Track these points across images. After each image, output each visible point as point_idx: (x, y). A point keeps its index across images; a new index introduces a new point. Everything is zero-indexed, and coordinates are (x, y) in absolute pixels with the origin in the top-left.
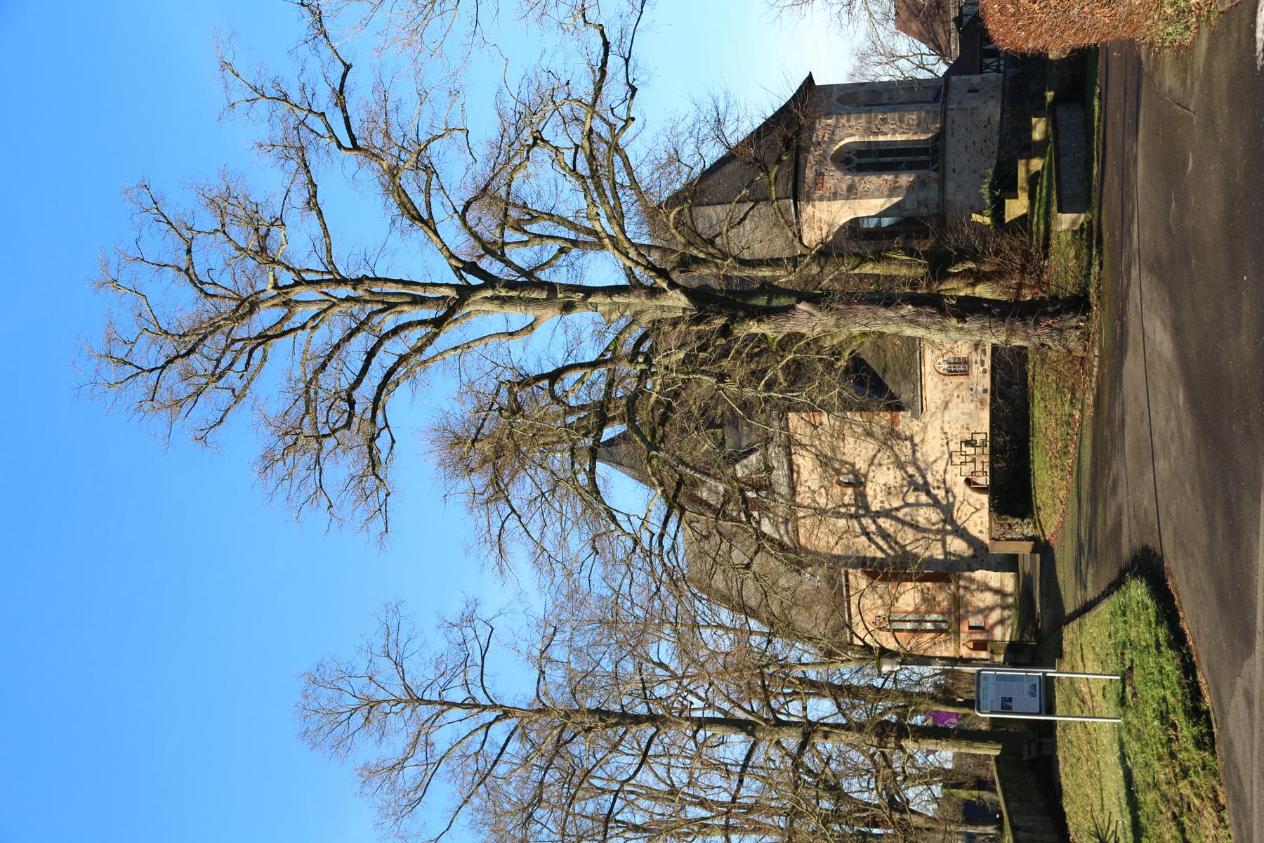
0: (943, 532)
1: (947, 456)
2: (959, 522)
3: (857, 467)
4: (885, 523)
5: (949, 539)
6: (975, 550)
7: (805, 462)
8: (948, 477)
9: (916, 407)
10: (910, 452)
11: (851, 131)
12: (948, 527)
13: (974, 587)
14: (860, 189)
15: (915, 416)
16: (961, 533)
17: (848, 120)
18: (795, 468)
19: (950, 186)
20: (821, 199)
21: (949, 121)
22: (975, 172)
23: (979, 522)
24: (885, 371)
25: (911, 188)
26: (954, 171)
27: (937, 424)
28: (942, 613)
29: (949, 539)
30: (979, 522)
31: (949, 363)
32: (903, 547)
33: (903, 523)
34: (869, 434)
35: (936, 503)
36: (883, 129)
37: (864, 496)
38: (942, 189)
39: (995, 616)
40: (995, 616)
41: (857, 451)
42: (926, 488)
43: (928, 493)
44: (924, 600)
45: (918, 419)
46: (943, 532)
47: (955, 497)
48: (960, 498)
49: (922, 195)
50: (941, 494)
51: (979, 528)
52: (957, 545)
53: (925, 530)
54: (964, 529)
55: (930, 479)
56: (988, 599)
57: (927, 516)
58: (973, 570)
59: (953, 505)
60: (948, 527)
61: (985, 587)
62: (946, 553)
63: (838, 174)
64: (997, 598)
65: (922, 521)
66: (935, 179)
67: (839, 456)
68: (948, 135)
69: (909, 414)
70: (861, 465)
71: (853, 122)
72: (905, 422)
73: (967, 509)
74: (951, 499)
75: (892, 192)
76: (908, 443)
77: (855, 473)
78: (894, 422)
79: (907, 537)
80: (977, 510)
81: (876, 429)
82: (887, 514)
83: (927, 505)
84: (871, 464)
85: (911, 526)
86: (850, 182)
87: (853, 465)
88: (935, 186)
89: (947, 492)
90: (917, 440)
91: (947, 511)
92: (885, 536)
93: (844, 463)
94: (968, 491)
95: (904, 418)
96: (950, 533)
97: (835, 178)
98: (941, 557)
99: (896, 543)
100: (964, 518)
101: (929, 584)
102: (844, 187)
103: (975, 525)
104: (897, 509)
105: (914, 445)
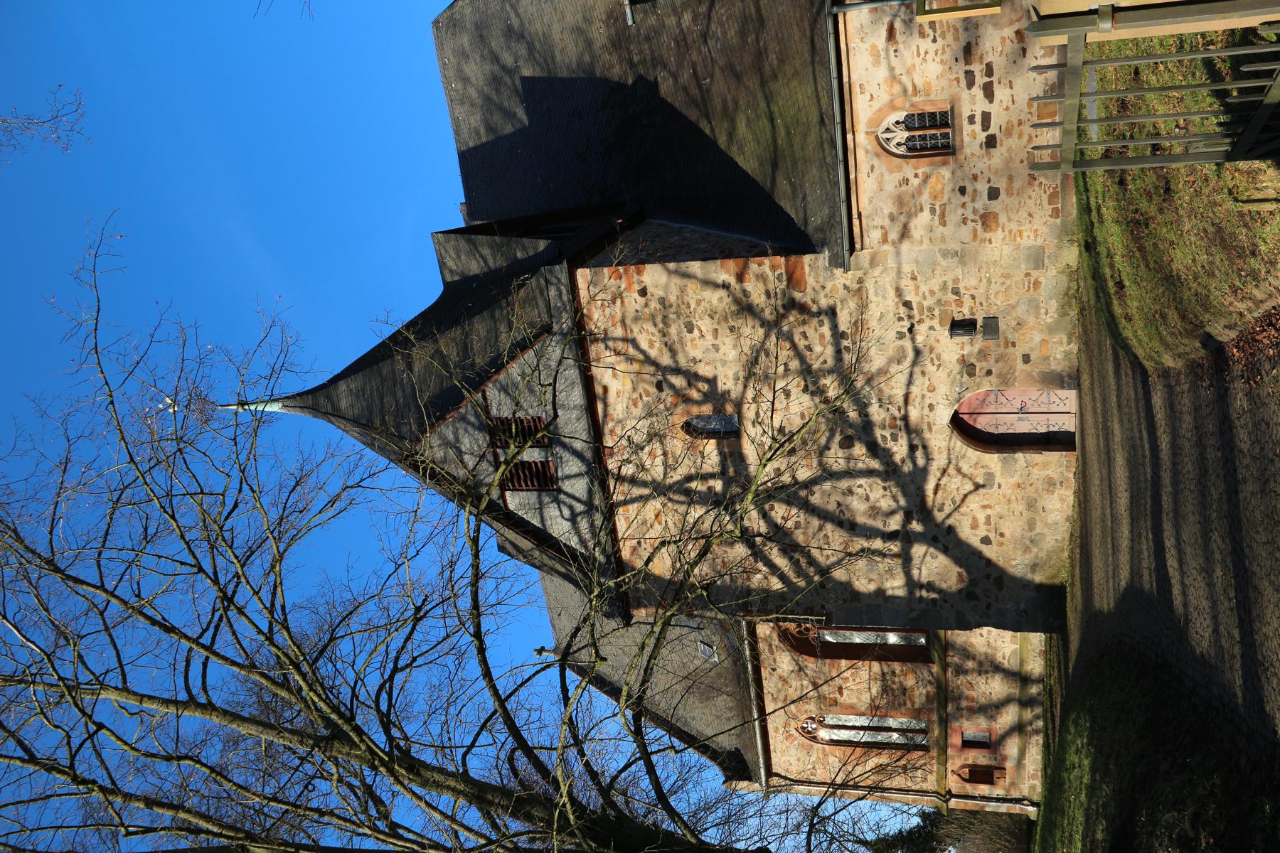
0: (905, 537)
1: (910, 355)
2: (939, 516)
3: (721, 386)
4: (779, 511)
5: (918, 550)
6: (972, 582)
7: (616, 381)
8: (914, 414)
9: (840, 239)
10: (830, 351)
12: (916, 526)
13: (970, 664)
15: (838, 262)
16: (944, 539)
18: (599, 390)
23: (981, 518)
24: (775, 165)
27: (887, 281)
28: (917, 714)
29: (918, 550)
30: (981, 518)
31: (908, 129)
32: (824, 571)
33: (824, 516)
34: (745, 308)
35: (890, 472)
37: (740, 458)
39: (1009, 717)
40: (1009, 717)
41: (719, 354)
42: (865, 431)
43: (874, 449)
44: (885, 690)
45: (842, 265)
46: (905, 537)
47: (928, 459)
48: (939, 461)
50: (899, 450)
51: (982, 532)
52: (933, 566)
53: (870, 533)
54: (951, 530)
55: (876, 413)
56: (996, 687)
57: (872, 498)
58: (967, 626)
59: (923, 473)
60: (916, 526)
61: (991, 666)
62: (912, 584)
64: (1014, 690)
65: (858, 507)
67: (683, 362)
69: (823, 258)
70: (728, 382)
72: (820, 278)
73: (955, 485)
74: (921, 462)
76: (826, 330)
77: (715, 396)
78: (793, 279)
79: (828, 544)
80: (978, 487)
81: (757, 296)
82: (793, 494)
83: (870, 473)
84: (749, 376)
85: (840, 523)
87: (712, 382)
89: (912, 448)
90: (844, 323)
91: (910, 483)
92: (779, 534)
93: (692, 378)
94: (958, 444)
95: (812, 266)
96: (920, 538)
98: (901, 593)
99: (812, 561)
100: (947, 509)
101: (897, 666)
103: (974, 526)
104: (809, 484)
105: (838, 335)
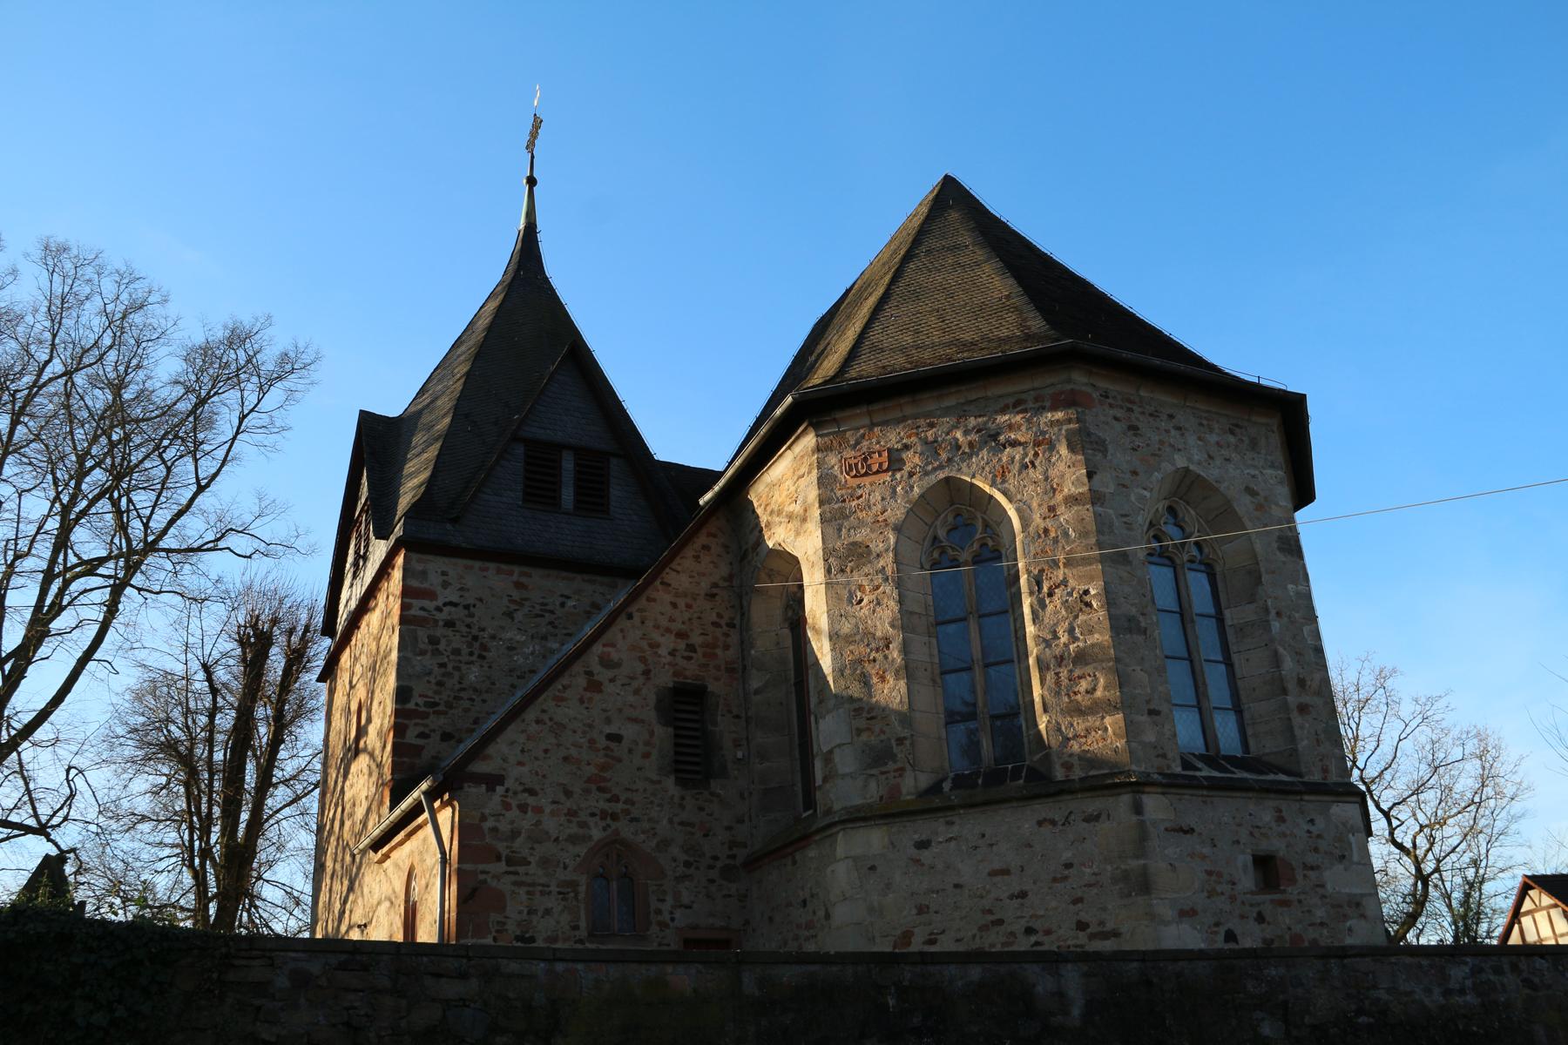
11: (1037, 520)
14: (858, 578)
17: (1072, 500)
19: (873, 839)
20: (825, 481)
21: (1093, 805)
22: (922, 910)
25: (864, 713)
26: (923, 845)
36: (1054, 605)
38: (859, 817)
49: (846, 762)
63: (897, 511)
66: (895, 791)
68: (1042, 809)
71: (1065, 515)
75: (855, 669)
86: (877, 546)
88: (874, 791)
97: (886, 502)
102: (860, 535)
